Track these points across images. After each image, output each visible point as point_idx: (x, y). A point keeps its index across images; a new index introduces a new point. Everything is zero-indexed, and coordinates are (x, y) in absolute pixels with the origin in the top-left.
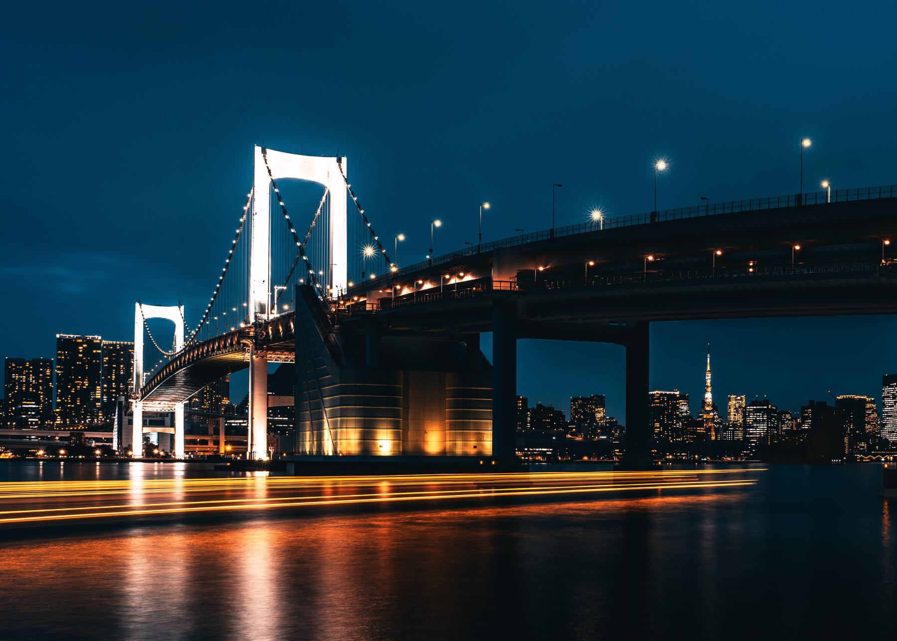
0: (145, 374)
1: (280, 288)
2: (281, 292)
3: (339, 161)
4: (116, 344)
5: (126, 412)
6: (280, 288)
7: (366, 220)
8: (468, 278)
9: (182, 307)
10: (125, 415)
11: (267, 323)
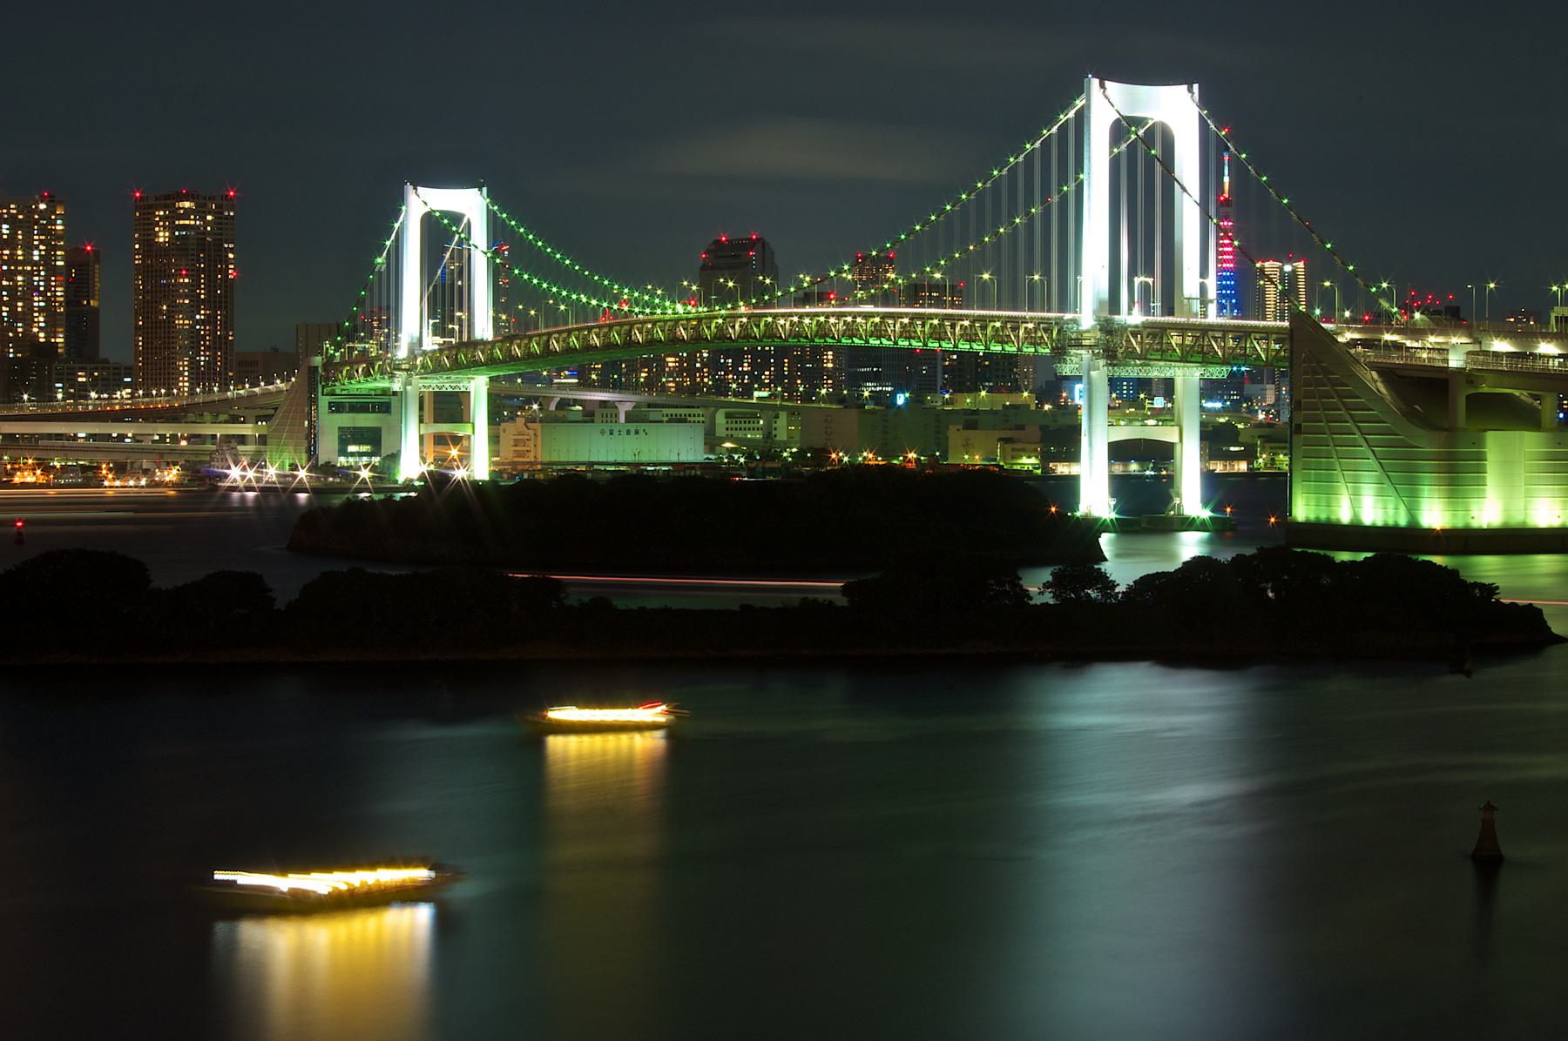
0: (431, 322)
3: (1190, 90)
5: (323, 387)
10: (323, 395)
11: (1124, 328)
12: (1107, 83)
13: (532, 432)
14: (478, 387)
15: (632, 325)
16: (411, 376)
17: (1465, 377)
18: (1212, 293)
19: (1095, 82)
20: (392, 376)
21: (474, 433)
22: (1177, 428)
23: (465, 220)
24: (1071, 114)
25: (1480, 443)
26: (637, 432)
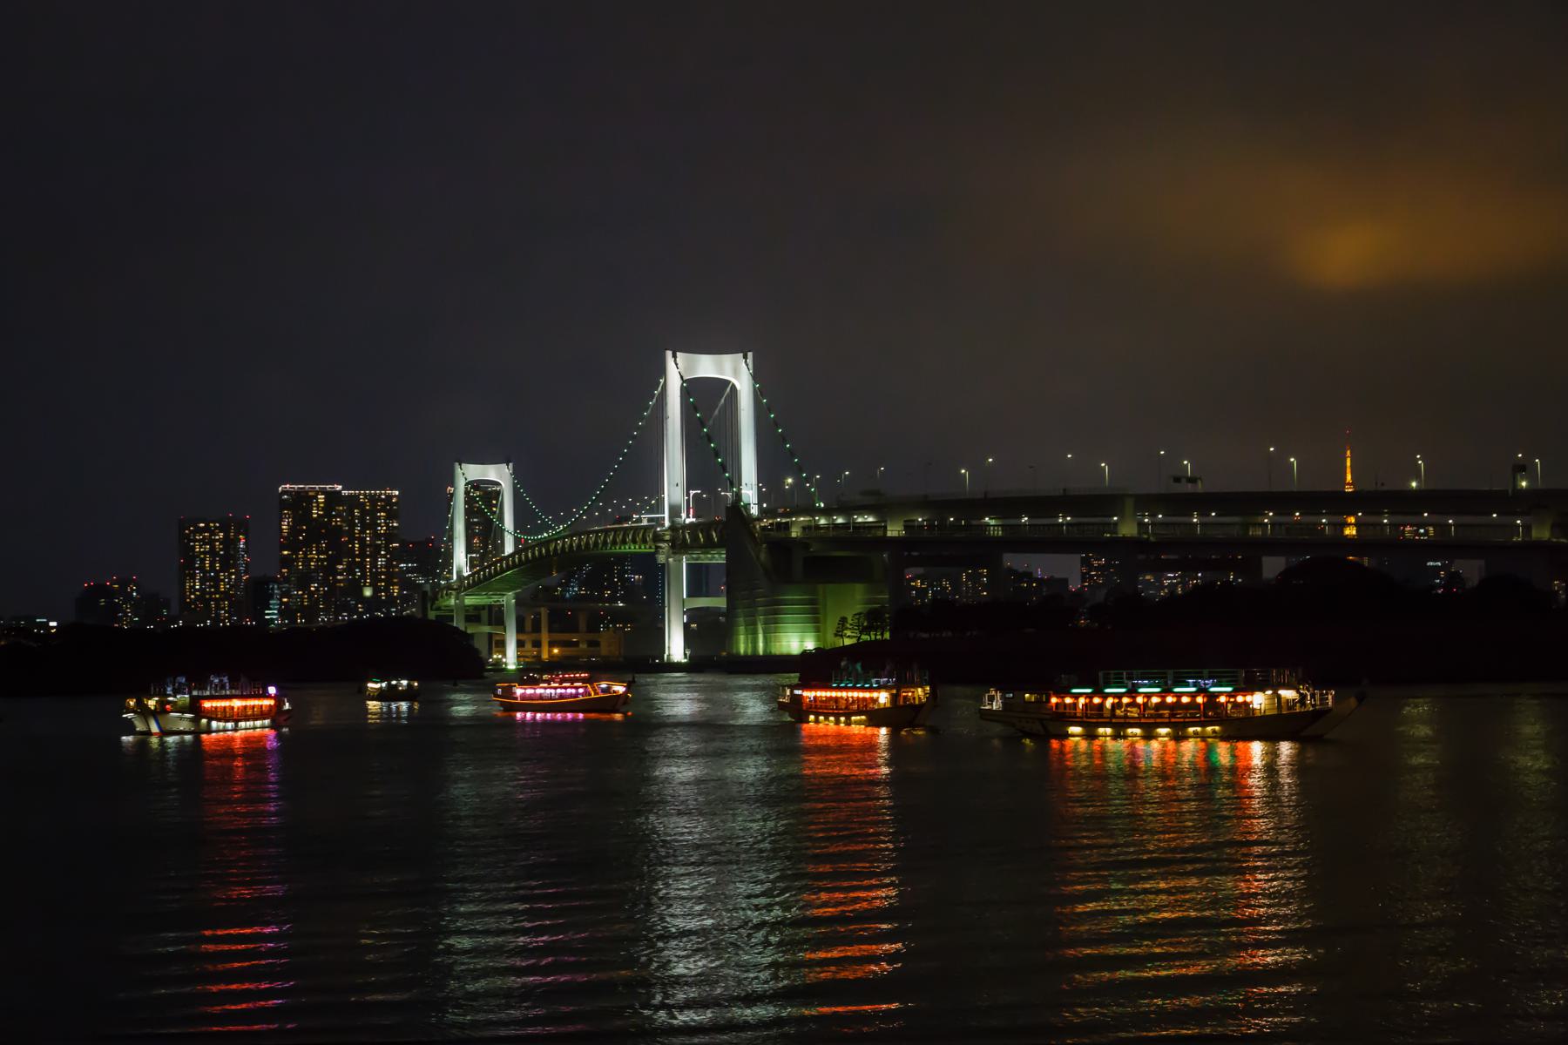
0: (469, 556)
1: (694, 492)
3: (745, 357)
4: (360, 494)
5: (431, 607)
6: (694, 492)
7: (785, 441)
8: (871, 519)
9: (511, 465)
10: (432, 609)
11: (685, 527)
12: (678, 354)
16: (458, 593)
17: (801, 543)
19: (669, 354)
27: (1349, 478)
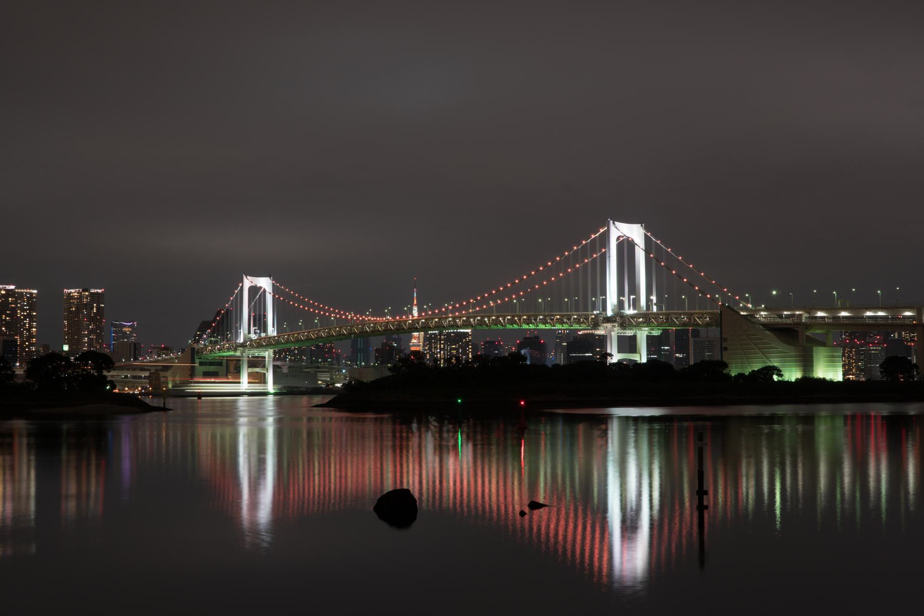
0: (254, 328)
2: (633, 299)
3: (642, 226)
5: (197, 356)
9: (271, 278)
11: (627, 316)
12: (615, 222)
13: (260, 376)
14: (268, 354)
15: (364, 325)
17: (807, 326)
18: (655, 301)
19: (611, 222)
20: (235, 350)
21: (267, 372)
22: (639, 355)
23: (262, 290)
24: (597, 235)
25: (812, 351)
26: (295, 376)
27: (415, 302)
